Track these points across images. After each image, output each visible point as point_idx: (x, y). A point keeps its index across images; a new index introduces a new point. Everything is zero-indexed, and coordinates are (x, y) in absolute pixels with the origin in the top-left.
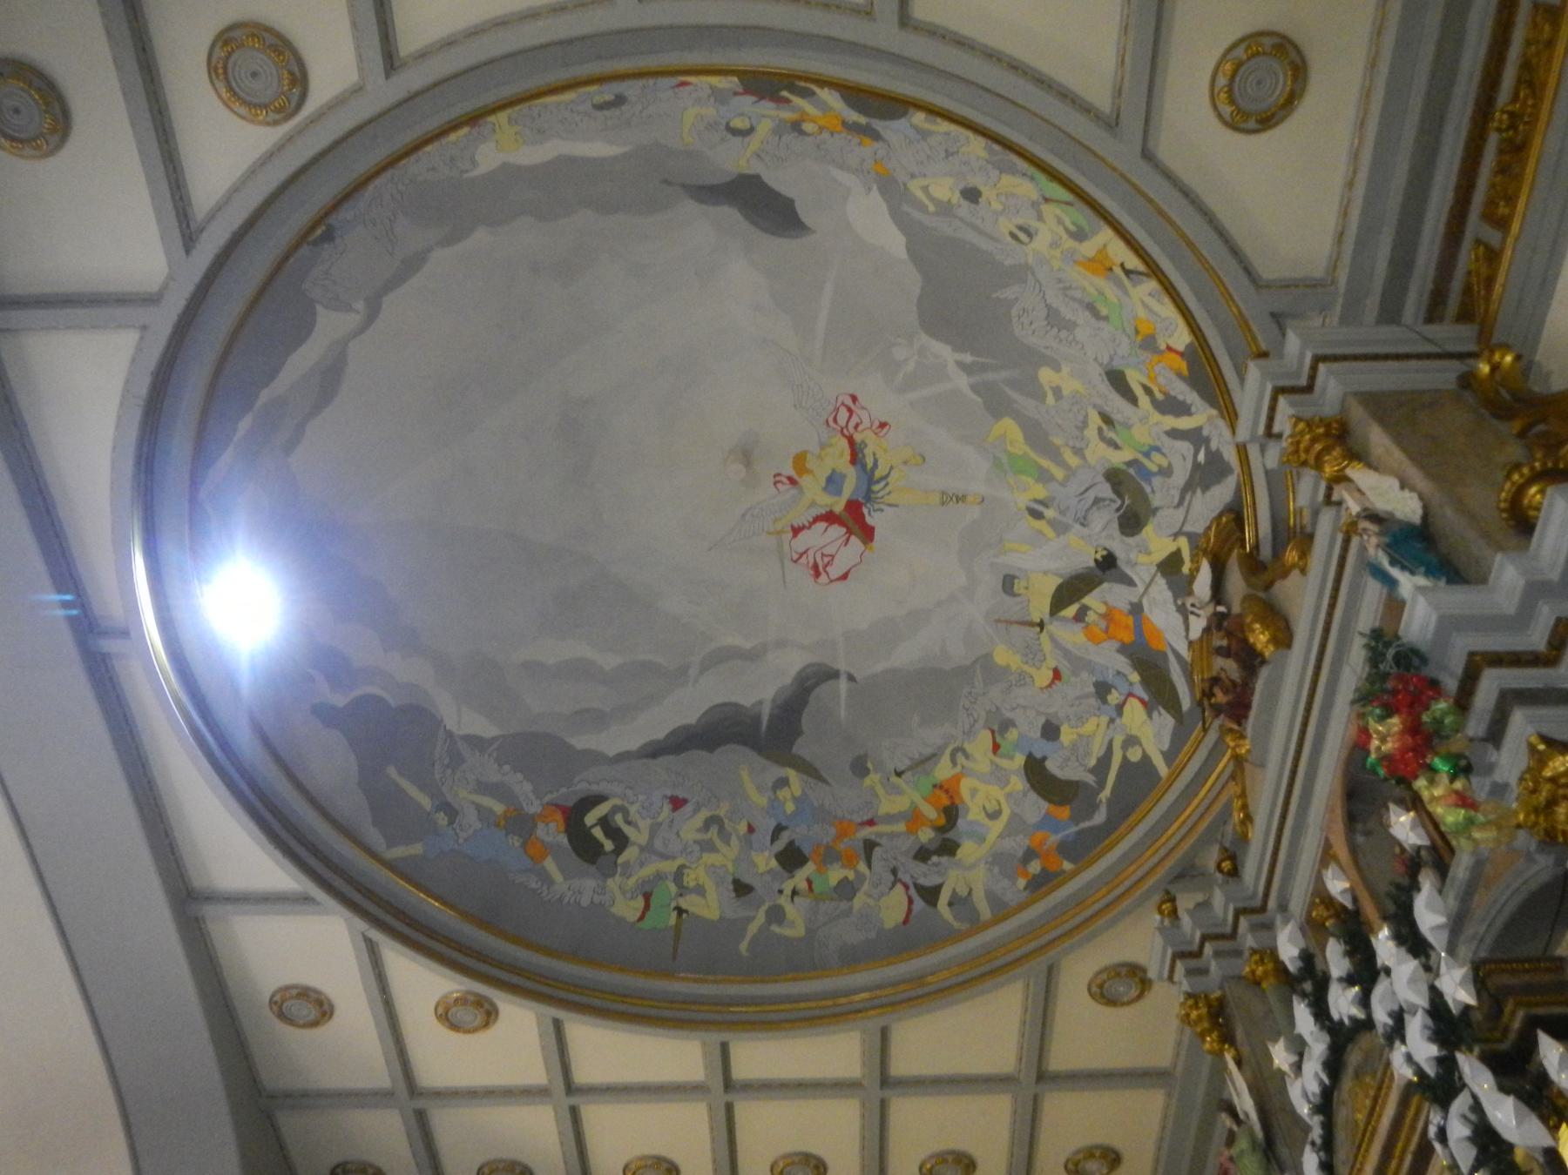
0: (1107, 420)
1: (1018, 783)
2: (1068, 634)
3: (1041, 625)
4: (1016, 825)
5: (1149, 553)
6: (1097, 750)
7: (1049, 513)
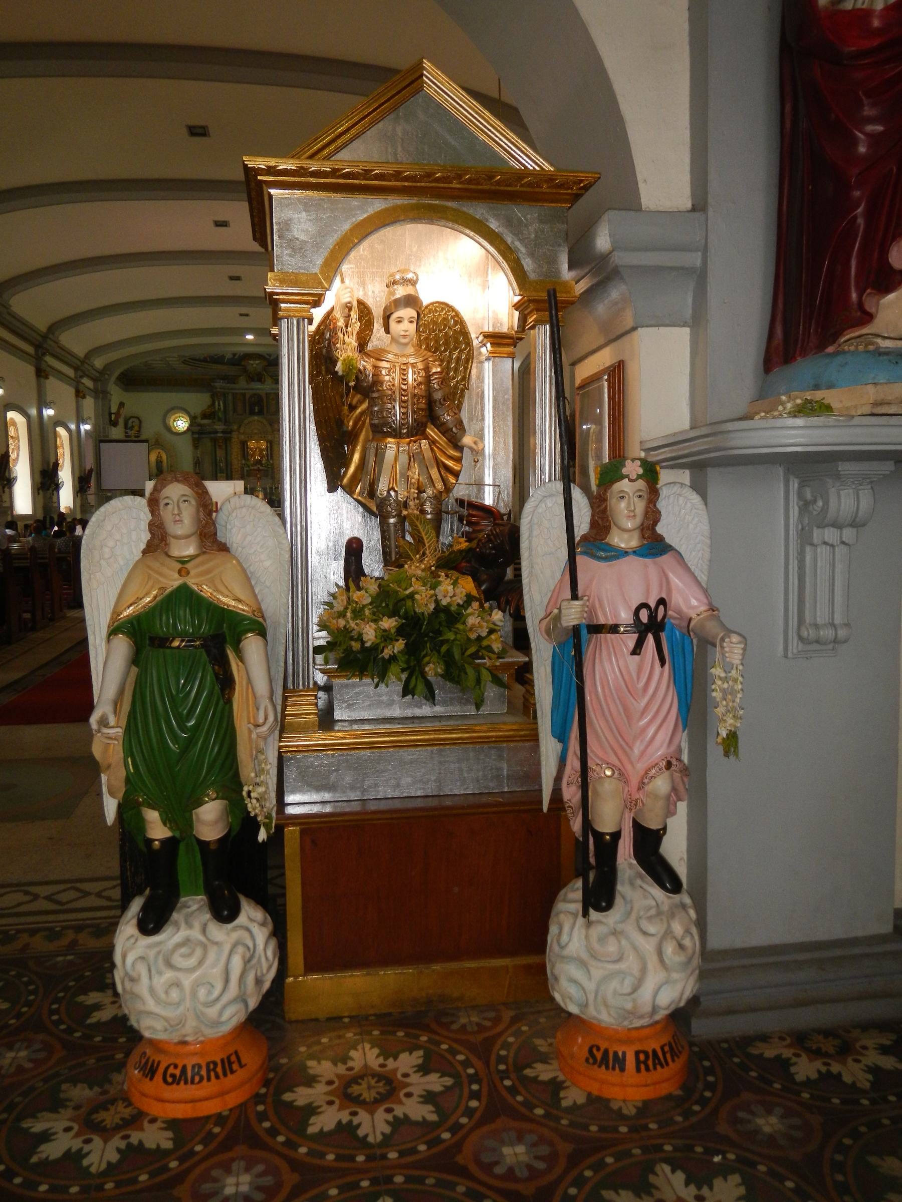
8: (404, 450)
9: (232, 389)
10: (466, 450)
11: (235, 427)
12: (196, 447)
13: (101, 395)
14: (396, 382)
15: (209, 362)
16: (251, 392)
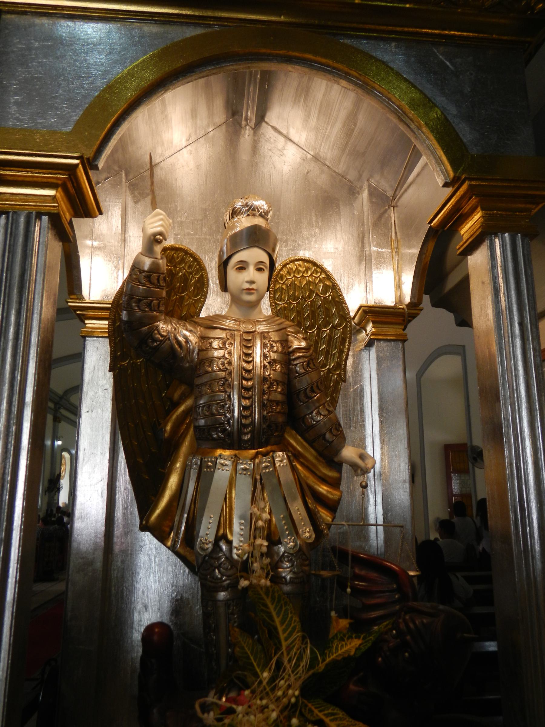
8: (245, 469)
10: (345, 467)
14: (235, 359)
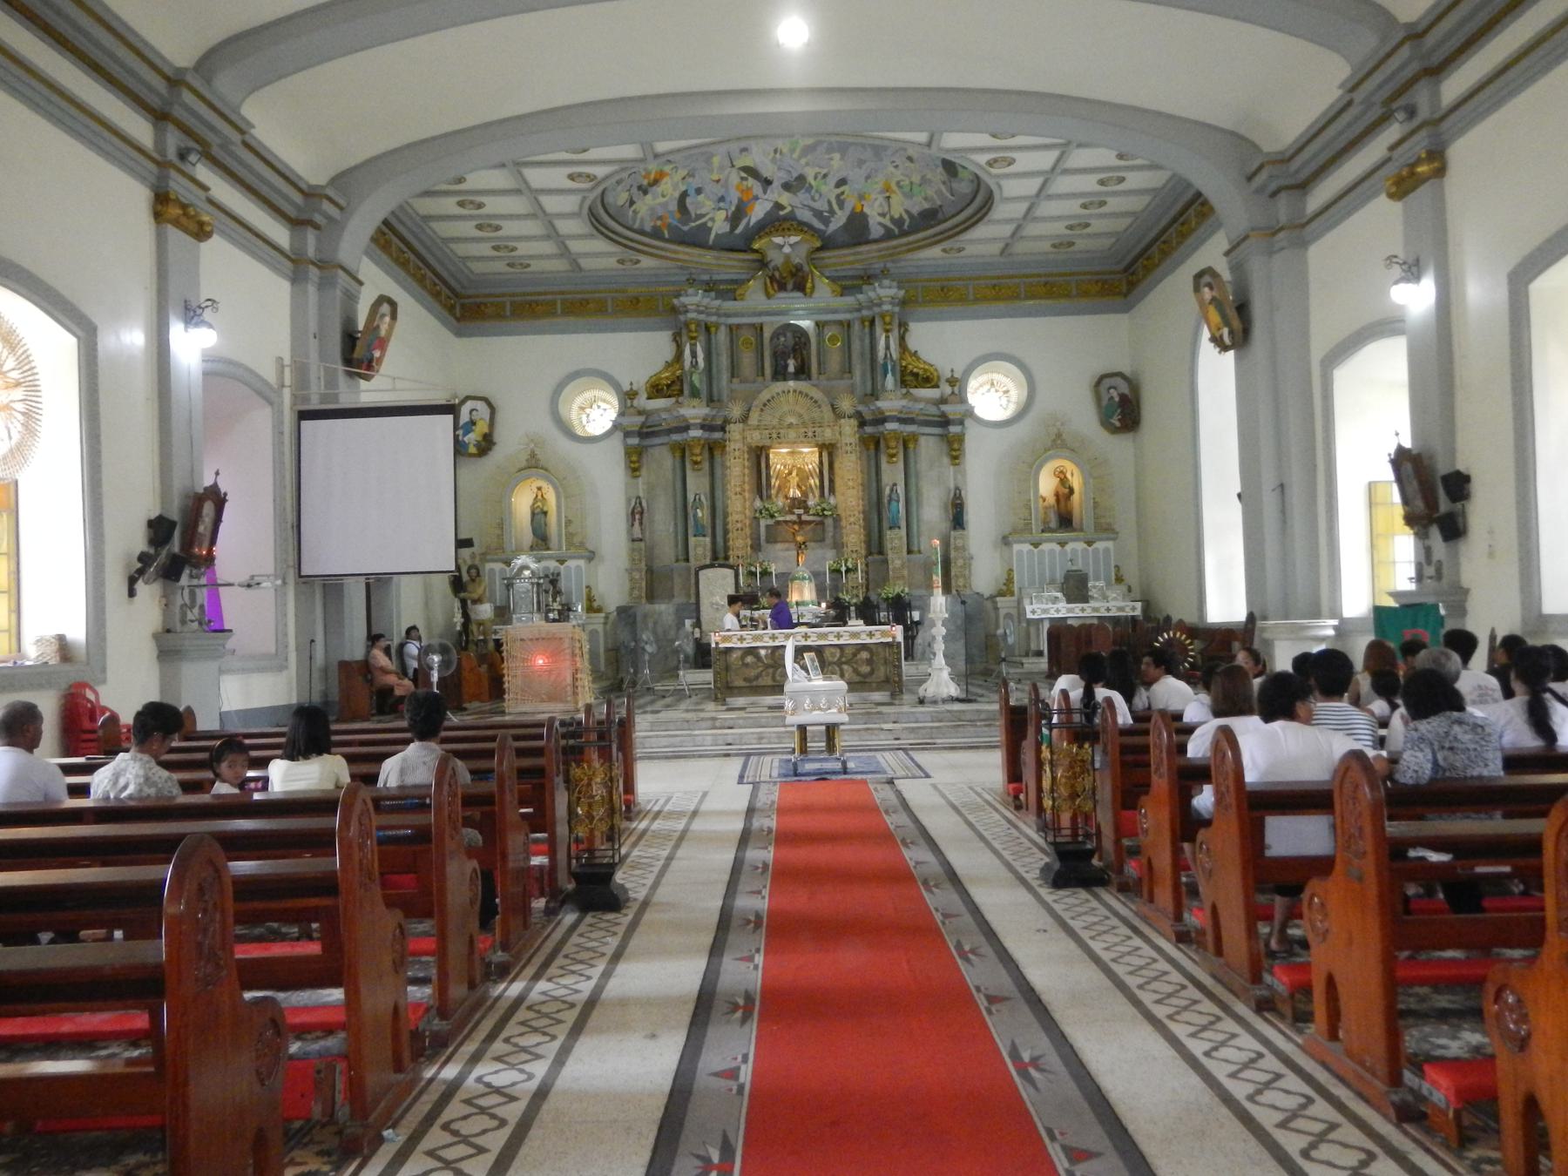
0: (825, 176)
1: (677, 195)
2: (734, 178)
3: (733, 166)
4: (665, 205)
5: (780, 195)
6: (703, 211)
7: (778, 156)
9: (728, 315)
11: (736, 411)
12: (634, 469)
13: (314, 272)
15: (667, 241)
16: (782, 320)
